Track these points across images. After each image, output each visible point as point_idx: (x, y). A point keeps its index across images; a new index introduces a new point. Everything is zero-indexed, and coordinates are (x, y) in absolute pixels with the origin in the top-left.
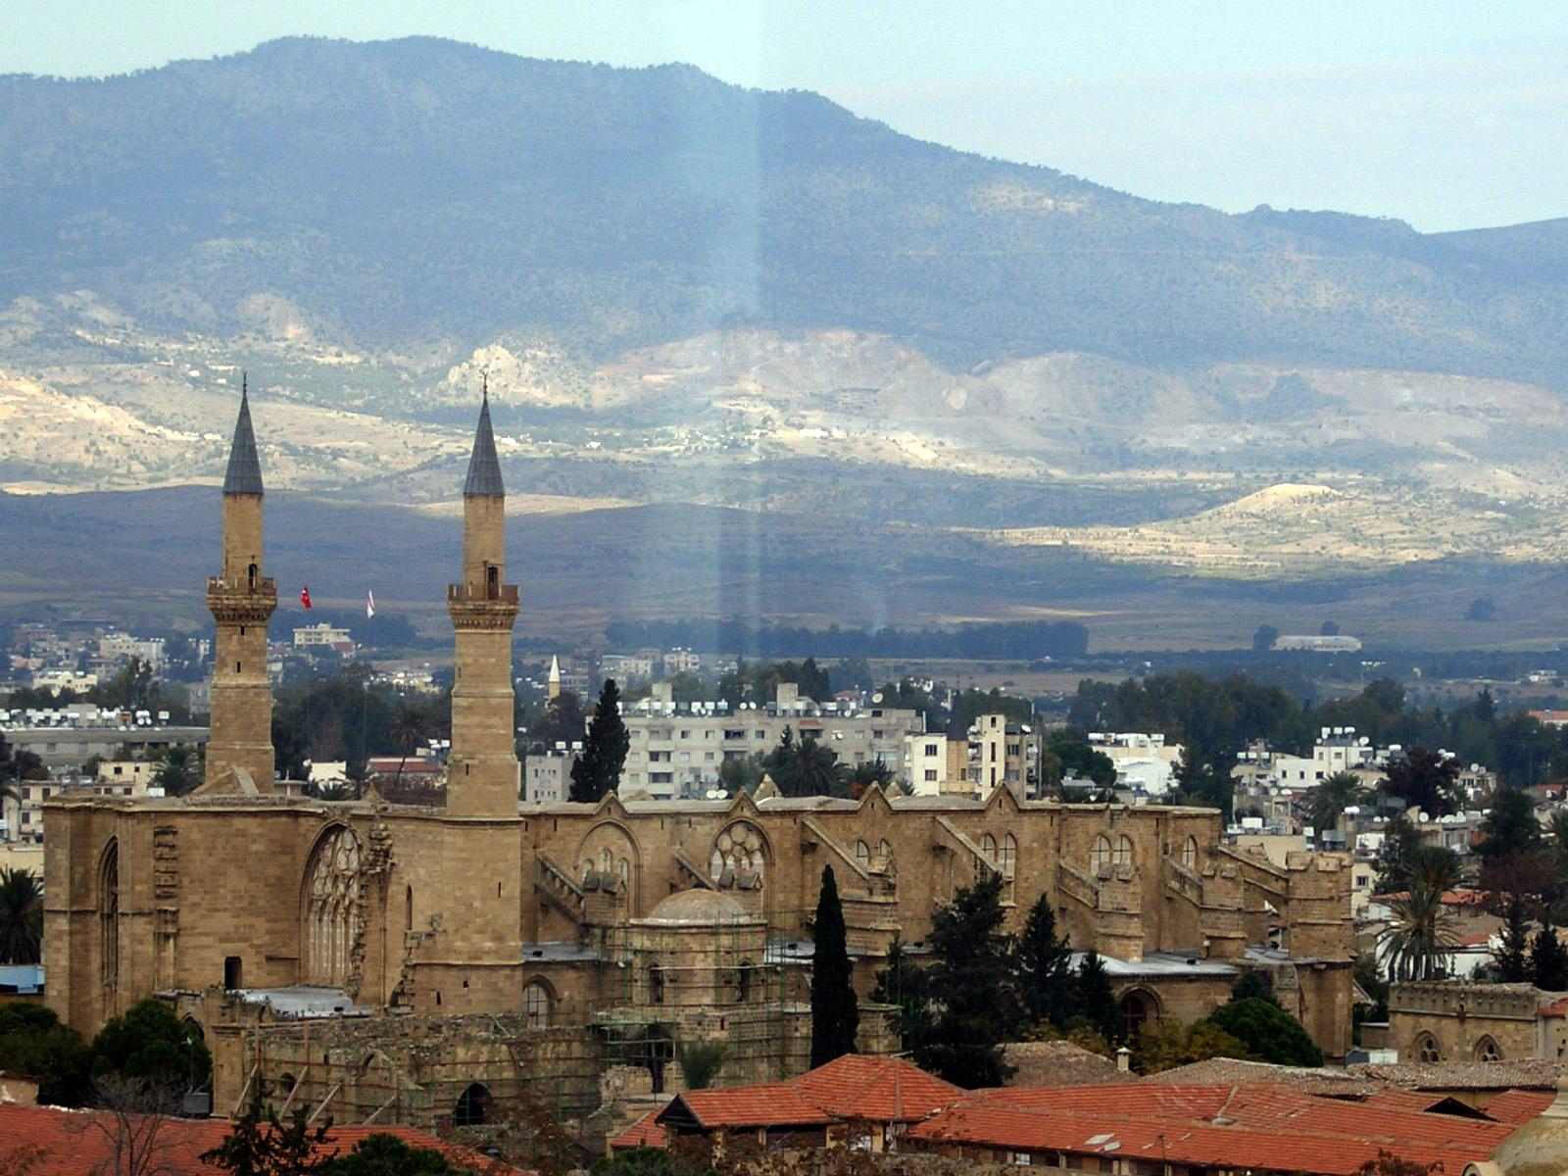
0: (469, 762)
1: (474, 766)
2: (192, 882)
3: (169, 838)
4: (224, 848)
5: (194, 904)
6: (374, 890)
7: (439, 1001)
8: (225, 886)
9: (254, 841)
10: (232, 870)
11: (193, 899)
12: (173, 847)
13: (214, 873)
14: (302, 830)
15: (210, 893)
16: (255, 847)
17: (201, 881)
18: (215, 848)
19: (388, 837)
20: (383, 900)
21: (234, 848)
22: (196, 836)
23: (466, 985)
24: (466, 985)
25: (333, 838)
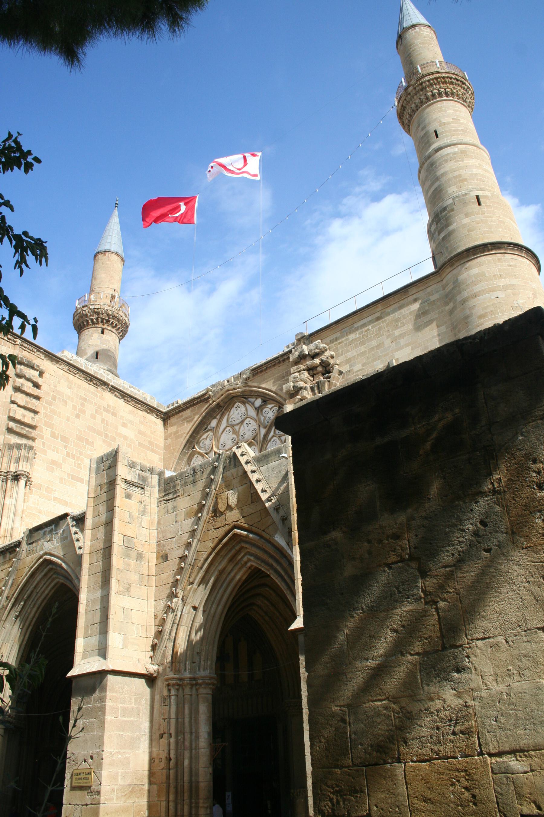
0: (480, 193)
1: (486, 197)
2: (53, 435)
3: (33, 374)
4: (93, 417)
5: (53, 462)
9: (124, 425)
11: (51, 455)
12: (36, 385)
15: (73, 457)
16: (123, 431)
17: (65, 439)
18: (84, 412)
21: (103, 421)
22: (63, 388)
25: (214, 423)
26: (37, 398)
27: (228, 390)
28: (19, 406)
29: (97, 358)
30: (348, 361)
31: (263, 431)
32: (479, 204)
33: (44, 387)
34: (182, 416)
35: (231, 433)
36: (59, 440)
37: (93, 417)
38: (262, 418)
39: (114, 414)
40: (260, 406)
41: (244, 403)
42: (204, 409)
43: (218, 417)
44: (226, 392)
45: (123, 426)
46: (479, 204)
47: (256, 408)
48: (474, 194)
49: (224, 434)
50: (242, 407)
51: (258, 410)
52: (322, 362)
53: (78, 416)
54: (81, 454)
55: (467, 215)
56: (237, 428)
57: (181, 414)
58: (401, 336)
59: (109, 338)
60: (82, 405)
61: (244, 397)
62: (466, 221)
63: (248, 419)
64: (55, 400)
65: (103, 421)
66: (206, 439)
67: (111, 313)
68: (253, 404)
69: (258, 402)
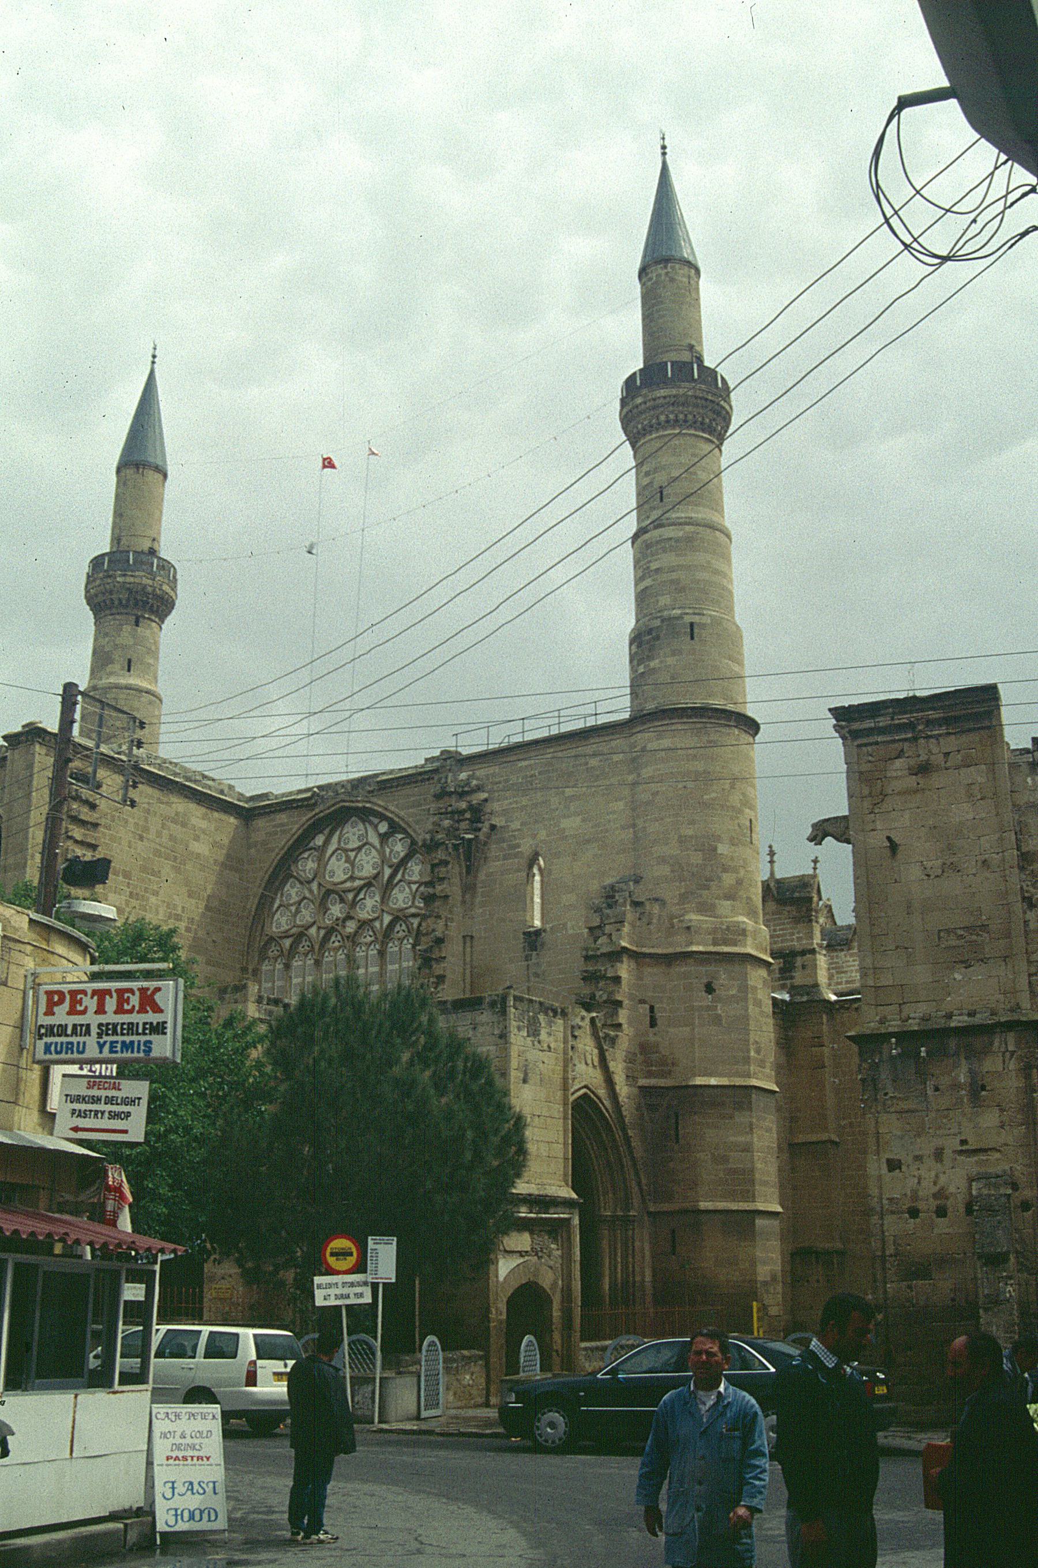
0: (696, 619)
1: (703, 626)
4: (159, 835)
6: (455, 870)
7: (653, 1023)
8: (156, 893)
9: (197, 838)
10: (166, 869)
13: (144, 869)
14: (258, 837)
16: (197, 847)
18: (146, 829)
19: (479, 789)
20: (469, 889)
21: (172, 838)
23: (709, 989)
24: (709, 989)
25: (319, 840)
26: (96, 825)
27: (344, 801)
28: (76, 842)
29: (129, 670)
30: (505, 812)
31: (388, 872)
32: (692, 638)
33: (103, 804)
34: (273, 820)
35: (344, 859)
36: (121, 878)
37: (159, 835)
38: (388, 850)
39: (184, 825)
40: (386, 833)
41: (364, 821)
42: (305, 818)
43: (327, 832)
44: (339, 802)
45: (194, 840)
46: (692, 638)
47: (380, 835)
48: (688, 619)
49: (334, 858)
50: (361, 826)
51: (384, 838)
52: (471, 808)
53: (141, 838)
54: (146, 890)
55: (674, 653)
56: (352, 854)
57: (272, 816)
58: (572, 798)
59: (148, 632)
60: (146, 819)
61: (365, 815)
62: (670, 661)
63: (367, 847)
64: (113, 821)
65: (172, 838)
66: (307, 858)
67: (150, 589)
68: (376, 827)
69: (383, 827)
